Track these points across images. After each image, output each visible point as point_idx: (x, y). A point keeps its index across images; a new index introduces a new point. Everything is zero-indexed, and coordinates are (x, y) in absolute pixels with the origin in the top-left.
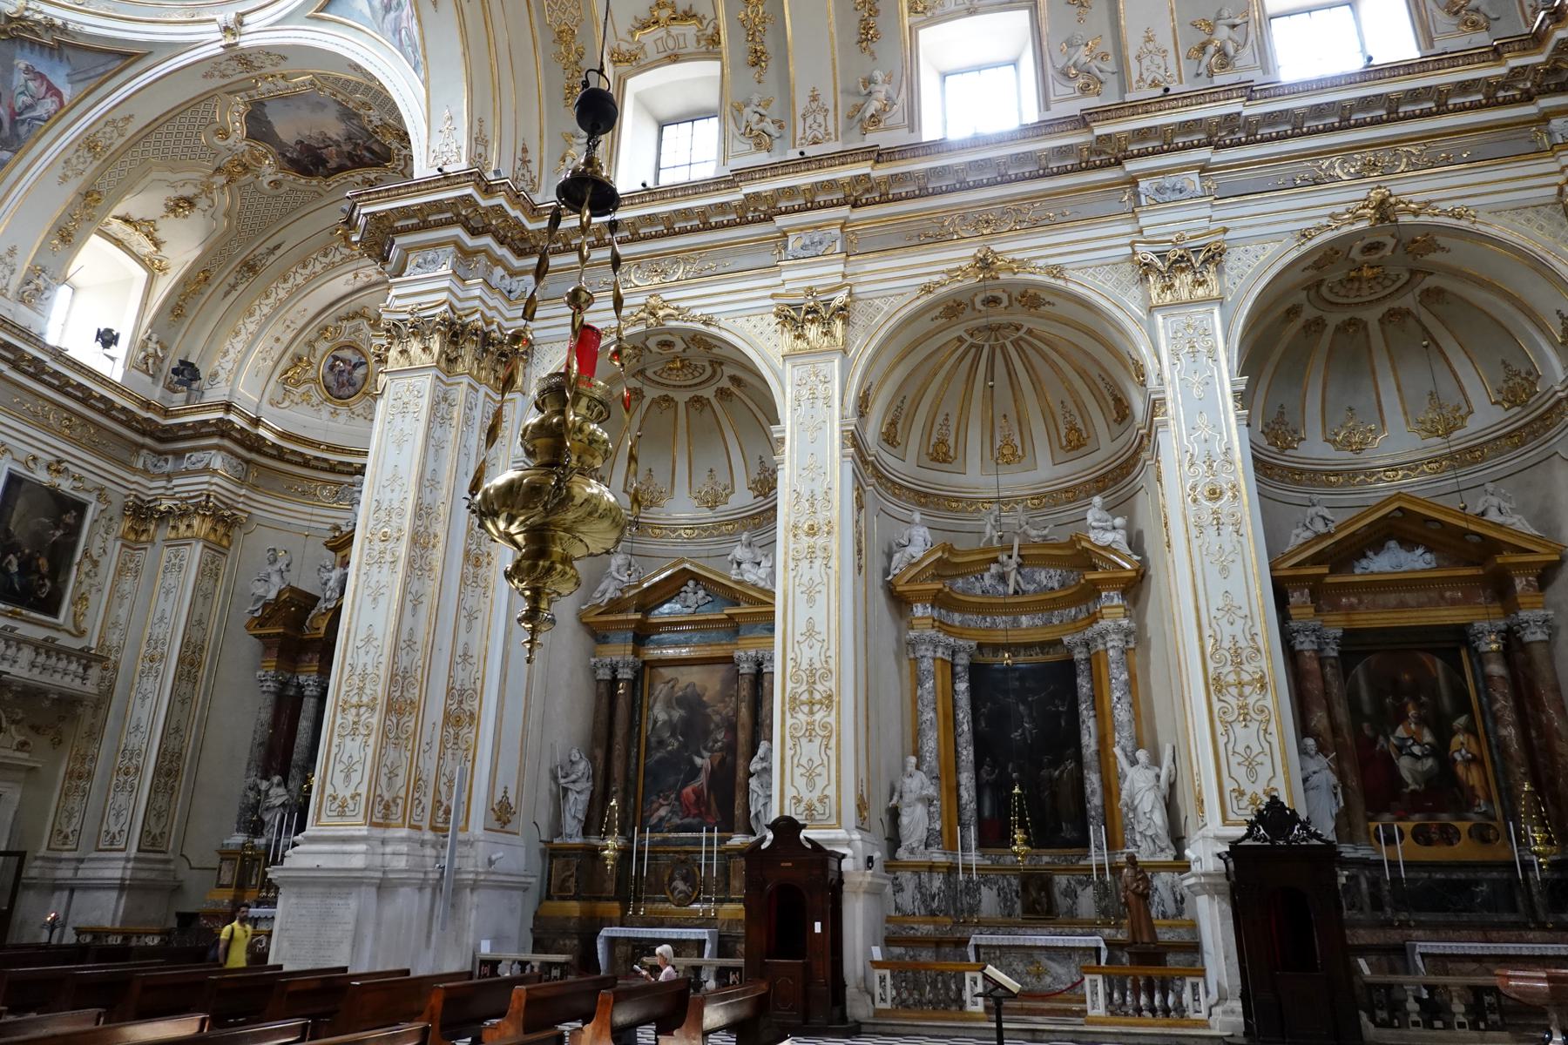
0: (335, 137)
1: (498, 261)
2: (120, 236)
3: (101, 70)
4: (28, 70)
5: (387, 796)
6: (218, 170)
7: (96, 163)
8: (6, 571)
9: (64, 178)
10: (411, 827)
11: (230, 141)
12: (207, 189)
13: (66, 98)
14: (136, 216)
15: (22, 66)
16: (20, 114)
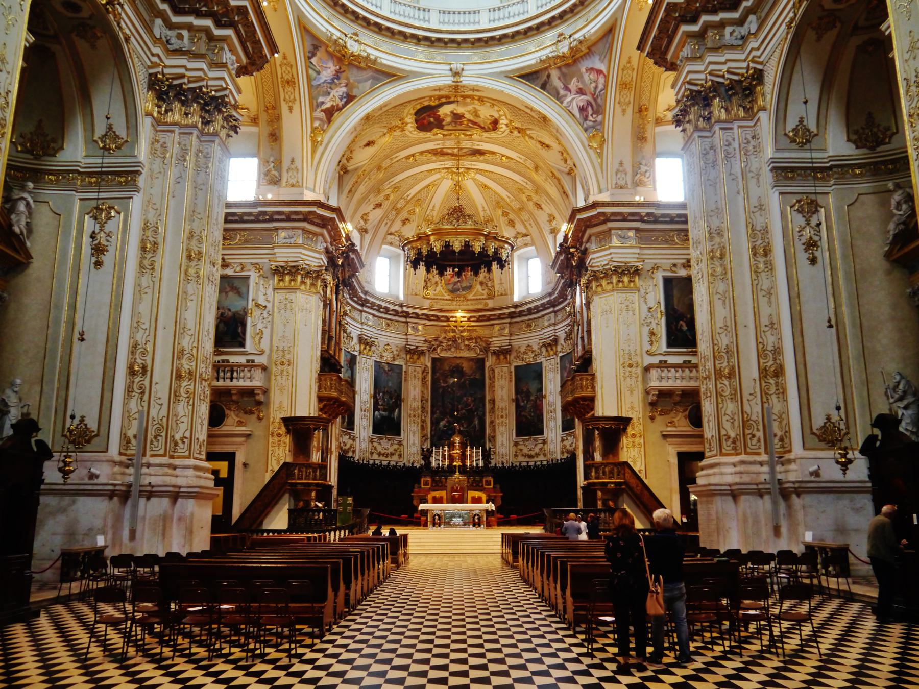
1: (722, 25)
4: (587, 70)
5: (733, 435)
8: (681, 330)
9: (624, 111)
10: (746, 453)
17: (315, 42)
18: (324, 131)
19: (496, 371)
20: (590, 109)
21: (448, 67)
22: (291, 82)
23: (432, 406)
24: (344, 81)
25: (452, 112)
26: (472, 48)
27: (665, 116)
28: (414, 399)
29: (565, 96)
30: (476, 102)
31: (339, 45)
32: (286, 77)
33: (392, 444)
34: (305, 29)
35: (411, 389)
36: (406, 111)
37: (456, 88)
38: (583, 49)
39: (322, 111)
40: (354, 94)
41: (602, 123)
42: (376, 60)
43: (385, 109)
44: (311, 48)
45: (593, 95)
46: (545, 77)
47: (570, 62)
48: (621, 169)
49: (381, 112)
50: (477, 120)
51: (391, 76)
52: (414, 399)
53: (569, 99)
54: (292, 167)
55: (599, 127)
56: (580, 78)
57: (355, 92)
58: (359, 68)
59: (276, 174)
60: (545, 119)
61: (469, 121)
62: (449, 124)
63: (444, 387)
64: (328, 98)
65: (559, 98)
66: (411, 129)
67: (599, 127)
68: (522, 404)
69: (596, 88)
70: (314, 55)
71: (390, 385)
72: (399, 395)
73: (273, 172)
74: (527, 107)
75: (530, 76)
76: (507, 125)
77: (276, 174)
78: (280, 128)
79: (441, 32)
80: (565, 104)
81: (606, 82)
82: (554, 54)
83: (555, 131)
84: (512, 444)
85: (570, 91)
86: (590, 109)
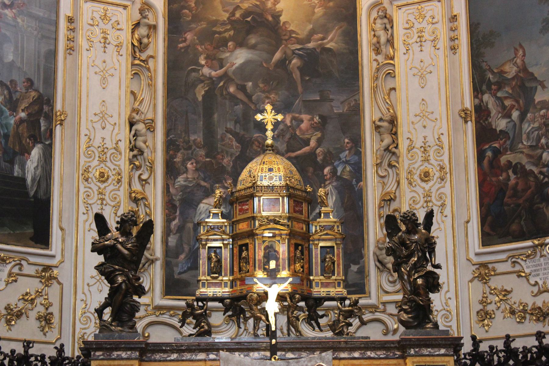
19: (400, 18)
23: (171, 146)
28: (103, 116)
33: (12, 278)
35: (90, 81)
52: (103, 116)
63: (212, 82)
68: (501, 124)
71: (10, 57)
72: (50, 101)
84: (468, 272)
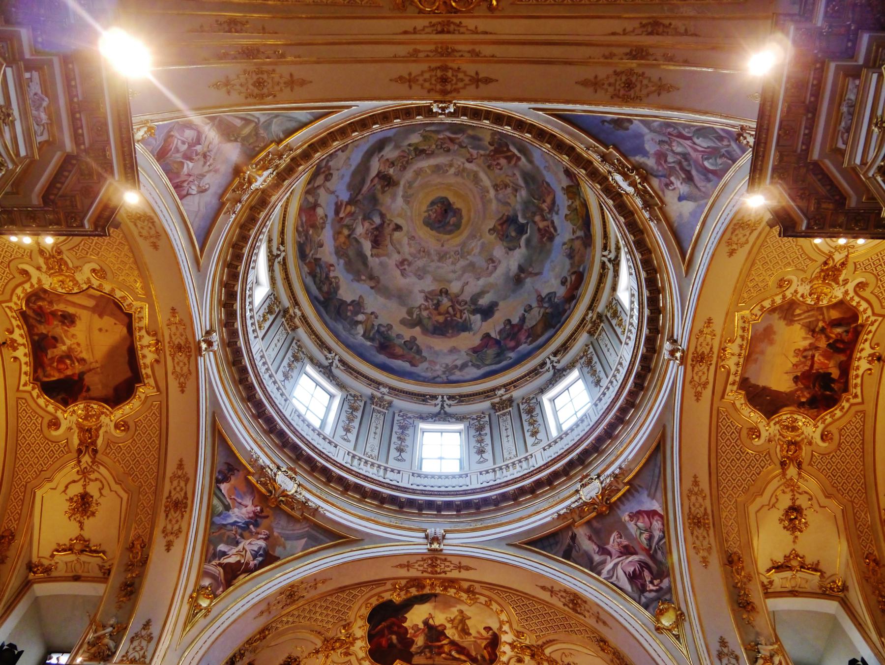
0: (806, 343)
2: (789, 586)
3: (657, 471)
4: (631, 517)
6: (783, 464)
7: (711, 532)
11: (764, 435)
12: (791, 486)
13: (660, 510)
14: (780, 559)
15: (627, 518)
16: (651, 547)
17: (231, 461)
18: (216, 596)
20: (646, 573)
21: (423, 535)
22: (180, 505)
24: (264, 532)
25: (426, 623)
26: (458, 516)
27: (771, 583)
29: (604, 562)
30: (464, 596)
31: (265, 475)
32: (176, 496)
34: (220, 436)
36: (356, 607)
37: (434, 558)
38: (620, 486)
39: (220, 565)
40: (277, 554)
41: (669, 590)
42: (316, 510)
43: (322, 588)
44: (224, 468)
45: (647, 551)
46: (568, 541)
47: (602, 514)
48: (725, 650)
49: (313, 593)
50: (466, 642)
51: (339, 537)
53: (609, 566)
54: (144, 633)
55: (667, 597)
56: (623, 530)
57: (278, 551)
58: (290, 517)
59: (112, 644)
60: (575, 601)
61: (453, 643)
62: (421, 652)
64: (234, 551)
65: (595, 568)
66: (362, 654)
67: (667, 597)
69: (650, 538)
70: (226, 479)
73: (107, 640)
74: (543, 588)
75: (543, 542)
76: (512, 646)
77: (112, 644)
78: (141, 576)
79: (414, 492)
80: (605, 572)
81: (665, 531)
82: (577, 504)
83: (592, 622)
85: (610, 554)
86: (646, 573)
